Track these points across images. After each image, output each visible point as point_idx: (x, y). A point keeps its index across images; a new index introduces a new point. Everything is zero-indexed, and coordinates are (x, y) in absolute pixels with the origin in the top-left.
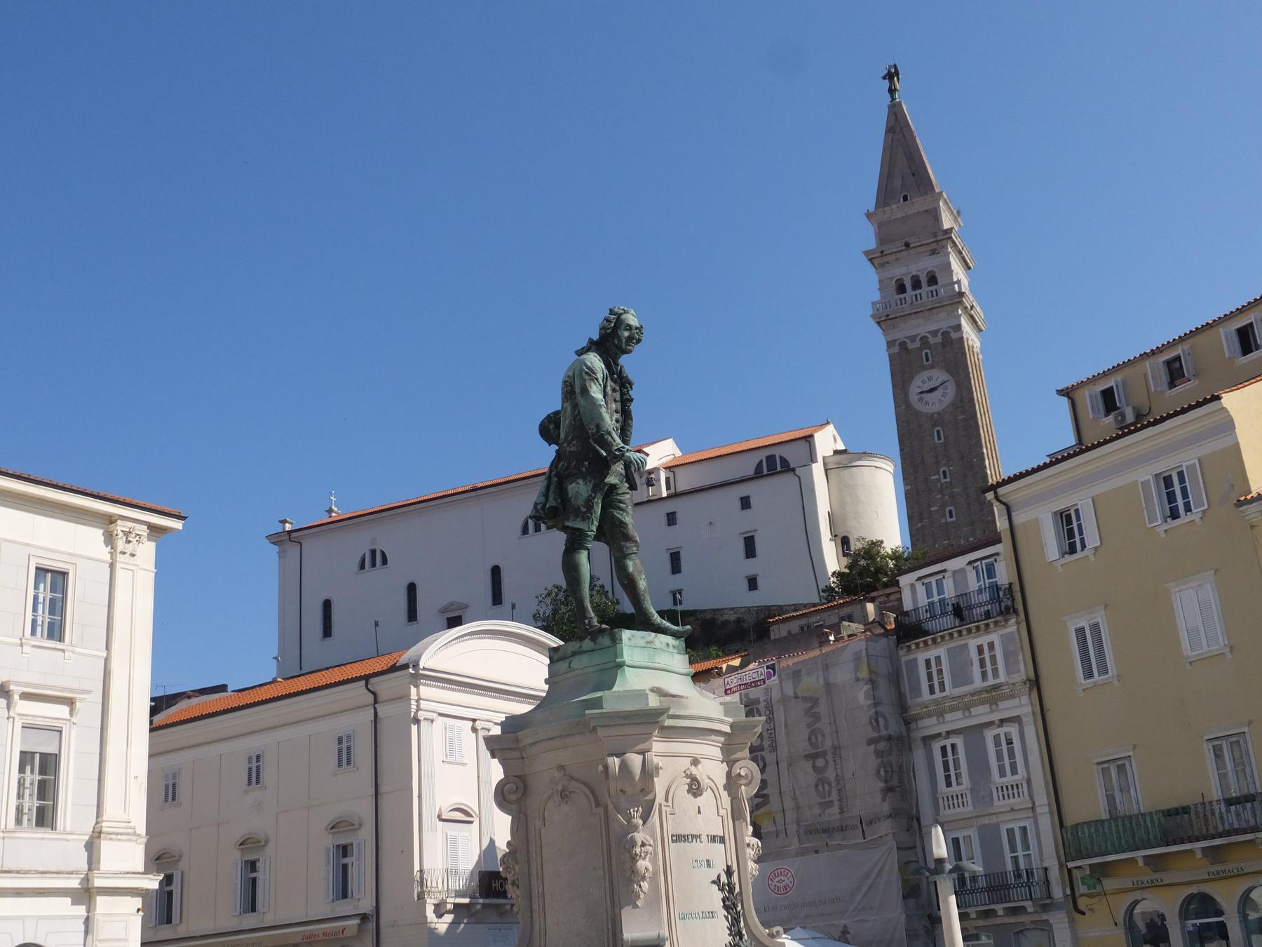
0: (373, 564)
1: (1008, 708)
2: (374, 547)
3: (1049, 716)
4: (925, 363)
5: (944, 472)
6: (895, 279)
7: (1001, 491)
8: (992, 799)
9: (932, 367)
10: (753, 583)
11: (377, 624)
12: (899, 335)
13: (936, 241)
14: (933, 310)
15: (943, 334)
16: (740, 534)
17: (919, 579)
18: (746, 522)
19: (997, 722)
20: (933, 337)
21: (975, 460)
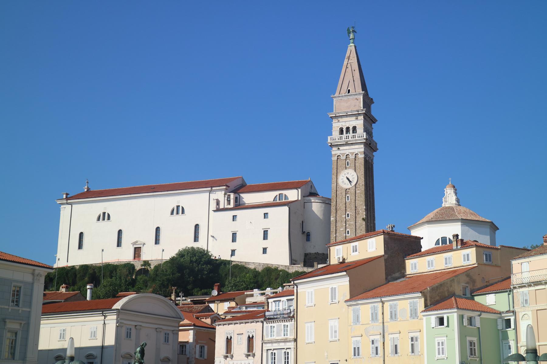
0: (104, 219)
2: (105, 211)
3: (298, 350)
4: (347, 166)
5: (348, 214)
6: (340, 127)
7: (295, 282)
10: (265, 250)
11: (103, 250)
12: (338, 153)
13: (358, 113)
14: (353, 144)
15: (356, 154)
16: (263, 229)
17: (274, 301)
19: (285, 349)
20: (351, 155)
21: (361, 211)
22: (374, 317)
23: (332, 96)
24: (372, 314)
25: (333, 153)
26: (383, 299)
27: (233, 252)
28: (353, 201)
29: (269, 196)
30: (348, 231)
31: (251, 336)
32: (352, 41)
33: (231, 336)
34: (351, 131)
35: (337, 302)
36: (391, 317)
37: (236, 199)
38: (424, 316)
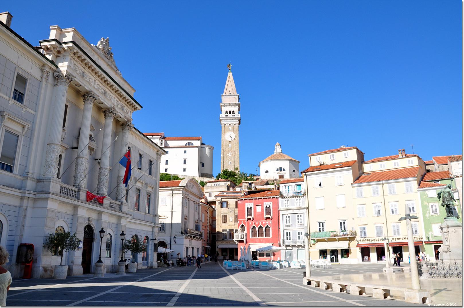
1: (301, 211)
3: (309, 214)
5: (230, 154)
8: (296, 227)
9: (231, 131)
10: (184, 170)
12: (225, 123)
15: (234, 124)
17: (285, 186)
18: (185, 156)
22: (376, 193)
23: (222, 95)
24: (374, 191)
25: (222, 123)
26: (384, 182)
27: (166, 170)
28: (233, 147)
29: (183, 143)
30: (230, 162)
31: (268, 206)
32: (230, 70)
33: (251, 207)
34: (232, 113)
35: (343, 185)
36: (390, 193)
37: (166, 143)
38: (418, 191)
